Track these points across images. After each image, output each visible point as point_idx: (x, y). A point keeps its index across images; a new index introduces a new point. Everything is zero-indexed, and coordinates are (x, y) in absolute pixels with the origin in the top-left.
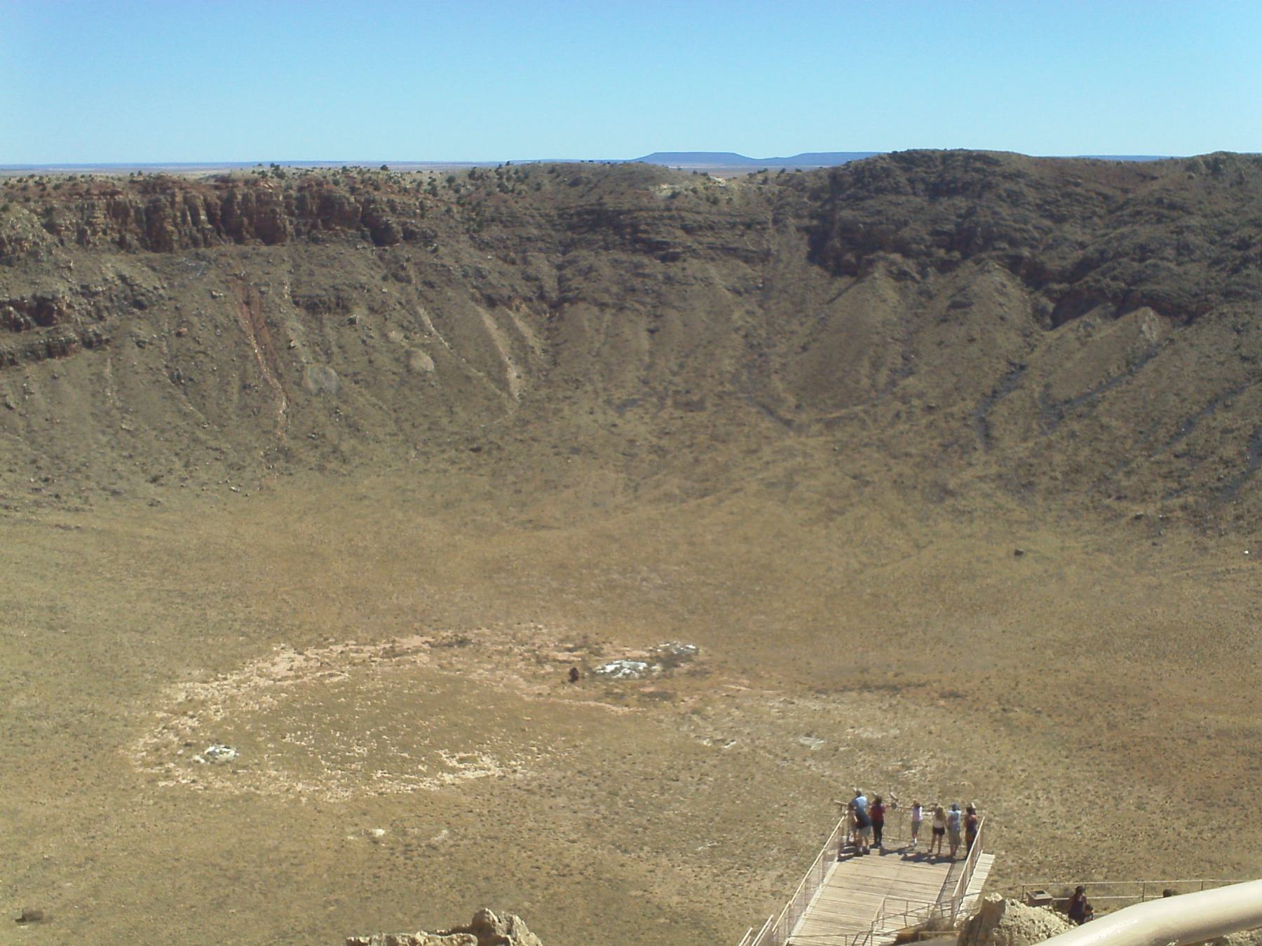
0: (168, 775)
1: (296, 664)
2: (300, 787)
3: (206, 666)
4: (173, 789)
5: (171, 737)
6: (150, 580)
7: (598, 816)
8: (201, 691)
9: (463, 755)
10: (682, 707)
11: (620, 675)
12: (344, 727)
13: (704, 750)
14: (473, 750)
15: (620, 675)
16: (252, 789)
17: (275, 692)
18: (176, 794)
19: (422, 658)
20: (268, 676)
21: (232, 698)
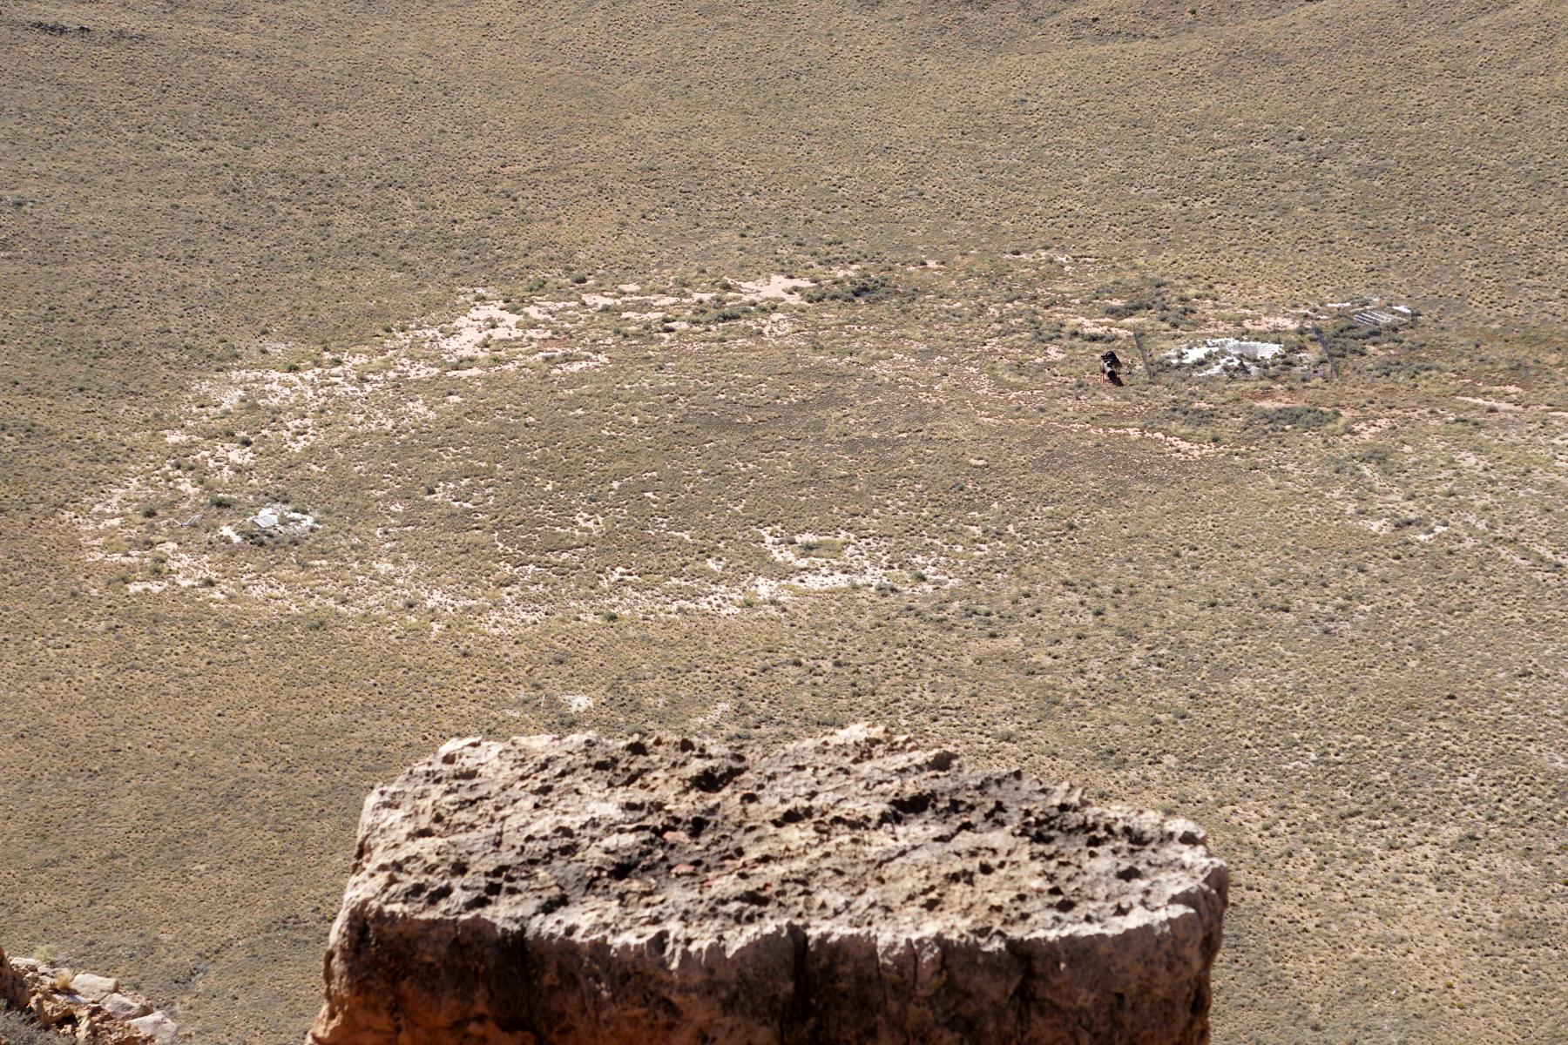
0: (157, 573)
1: (499, 333)
2: (435, 599)
3: (300, 332)
4: (159, 599)
5: (187, 486)
6: (224, 146)
7: (1079, 683)
8: (278, 387)
9: (808, 538)
10: (1345, 446)
11: (1216, 369)
12: (563, 474)
13: (1370, 543)
14: (835, 529)
15: (1216, 369)
16: (331, 603)
17: (436, 389)
18: (163, 610)
19: (778, 326)
20: (435, 359)
21: (342, 405)
